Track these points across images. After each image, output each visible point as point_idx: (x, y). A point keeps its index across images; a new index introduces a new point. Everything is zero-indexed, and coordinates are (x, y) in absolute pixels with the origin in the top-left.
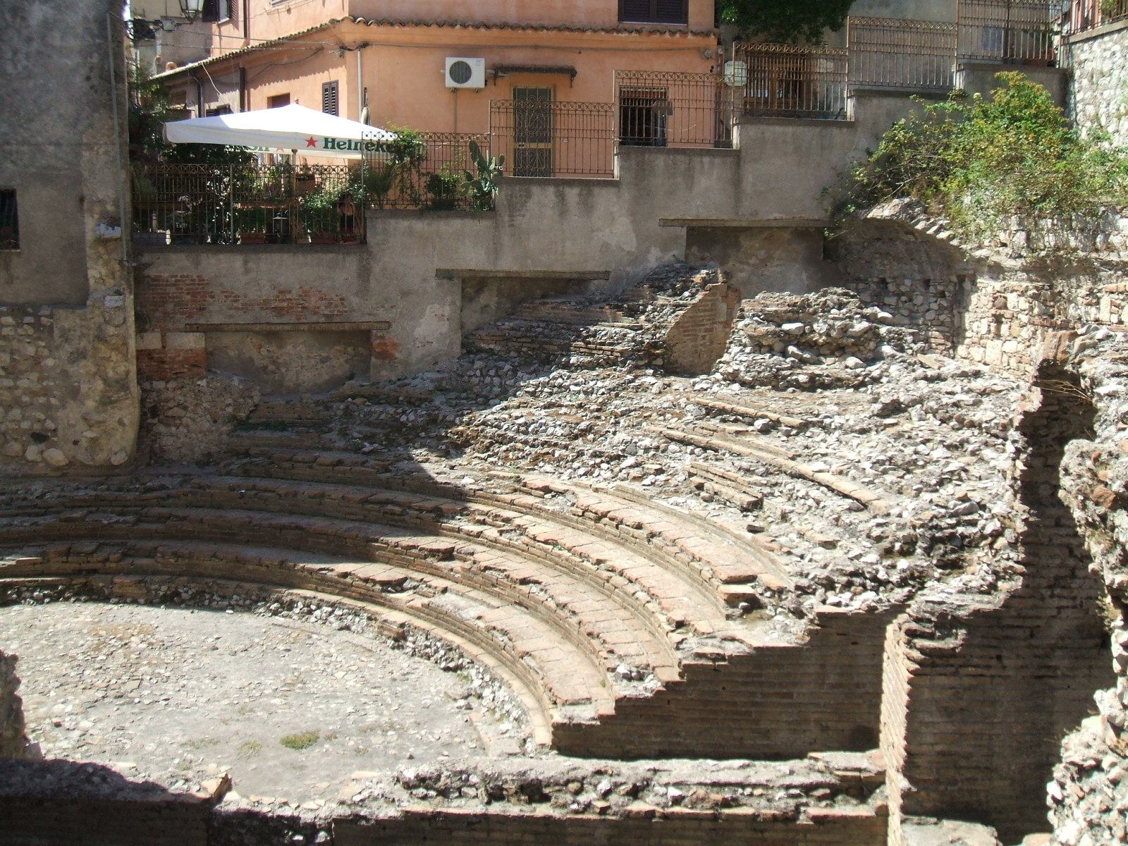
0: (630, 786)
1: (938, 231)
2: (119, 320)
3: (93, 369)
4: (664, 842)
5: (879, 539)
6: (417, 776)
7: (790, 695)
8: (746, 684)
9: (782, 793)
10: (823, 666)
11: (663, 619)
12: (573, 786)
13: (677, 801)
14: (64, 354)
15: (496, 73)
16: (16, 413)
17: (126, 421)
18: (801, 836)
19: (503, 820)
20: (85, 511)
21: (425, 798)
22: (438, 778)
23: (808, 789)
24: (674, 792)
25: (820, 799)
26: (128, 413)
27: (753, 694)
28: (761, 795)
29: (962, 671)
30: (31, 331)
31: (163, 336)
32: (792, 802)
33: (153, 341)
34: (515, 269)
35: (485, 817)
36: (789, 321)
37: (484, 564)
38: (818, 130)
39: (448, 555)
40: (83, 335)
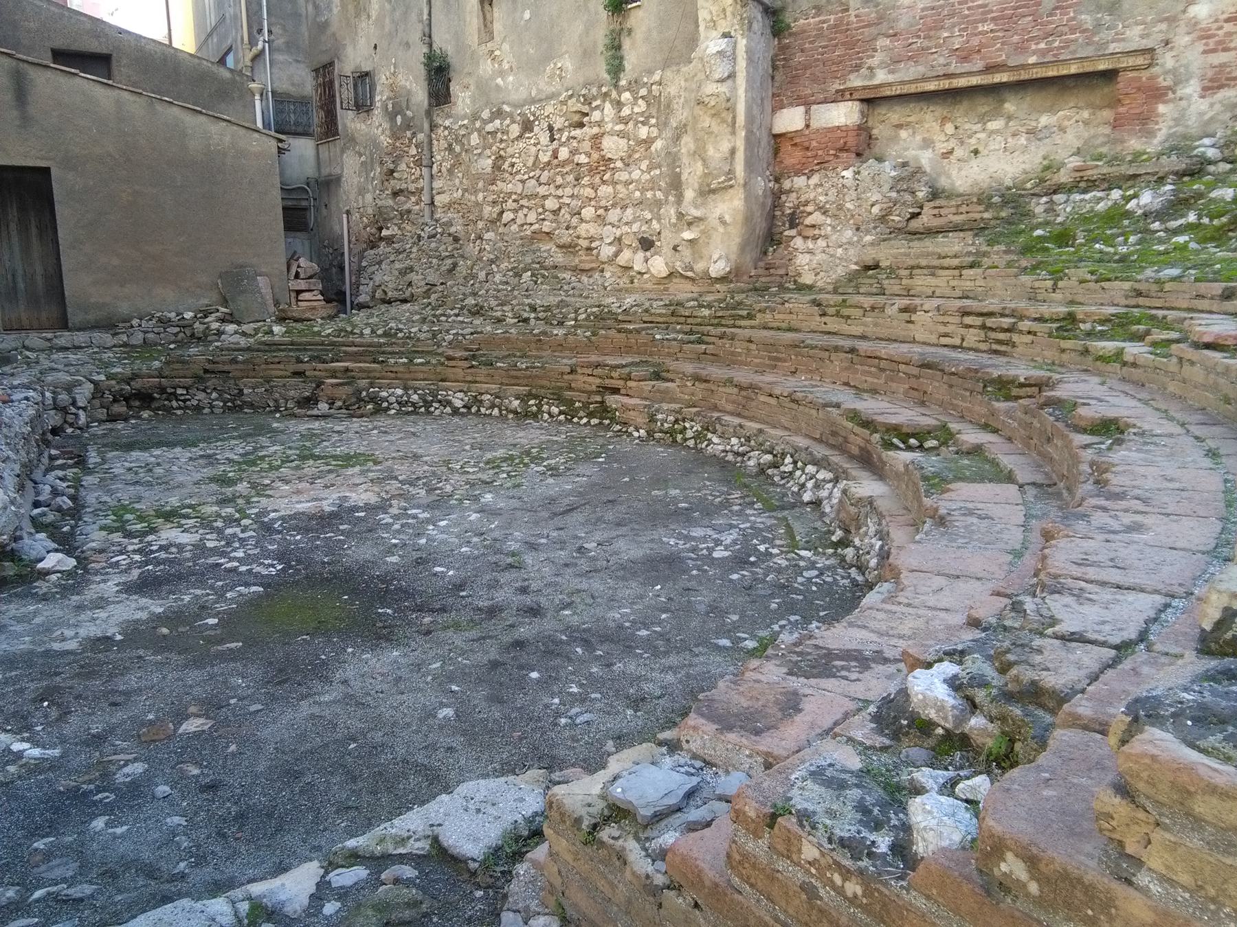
2: (721, 70)
14: (668, 133)
17: (727, 218)
31: (807, 112)
33: (790, 120)
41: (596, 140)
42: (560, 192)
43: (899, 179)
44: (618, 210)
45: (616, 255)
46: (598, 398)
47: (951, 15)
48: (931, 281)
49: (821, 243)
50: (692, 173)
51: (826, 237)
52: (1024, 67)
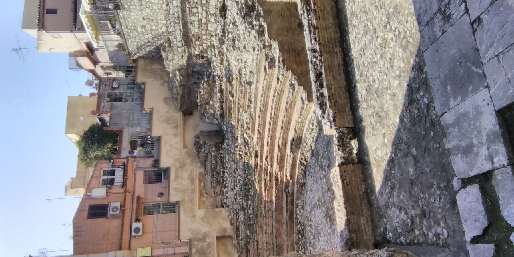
4: (326, 40)
5: (250, 32)
7: (291, 43)
9: (310, 16)
10: (282, 35)
11: (278, 85)
13: (315, 39)
15: (138, 220)
19: (327, 81)
22: (320, 103)
23: (308, 11)
24: (313, 42)
25: (310, 7)
35: (327, 85)
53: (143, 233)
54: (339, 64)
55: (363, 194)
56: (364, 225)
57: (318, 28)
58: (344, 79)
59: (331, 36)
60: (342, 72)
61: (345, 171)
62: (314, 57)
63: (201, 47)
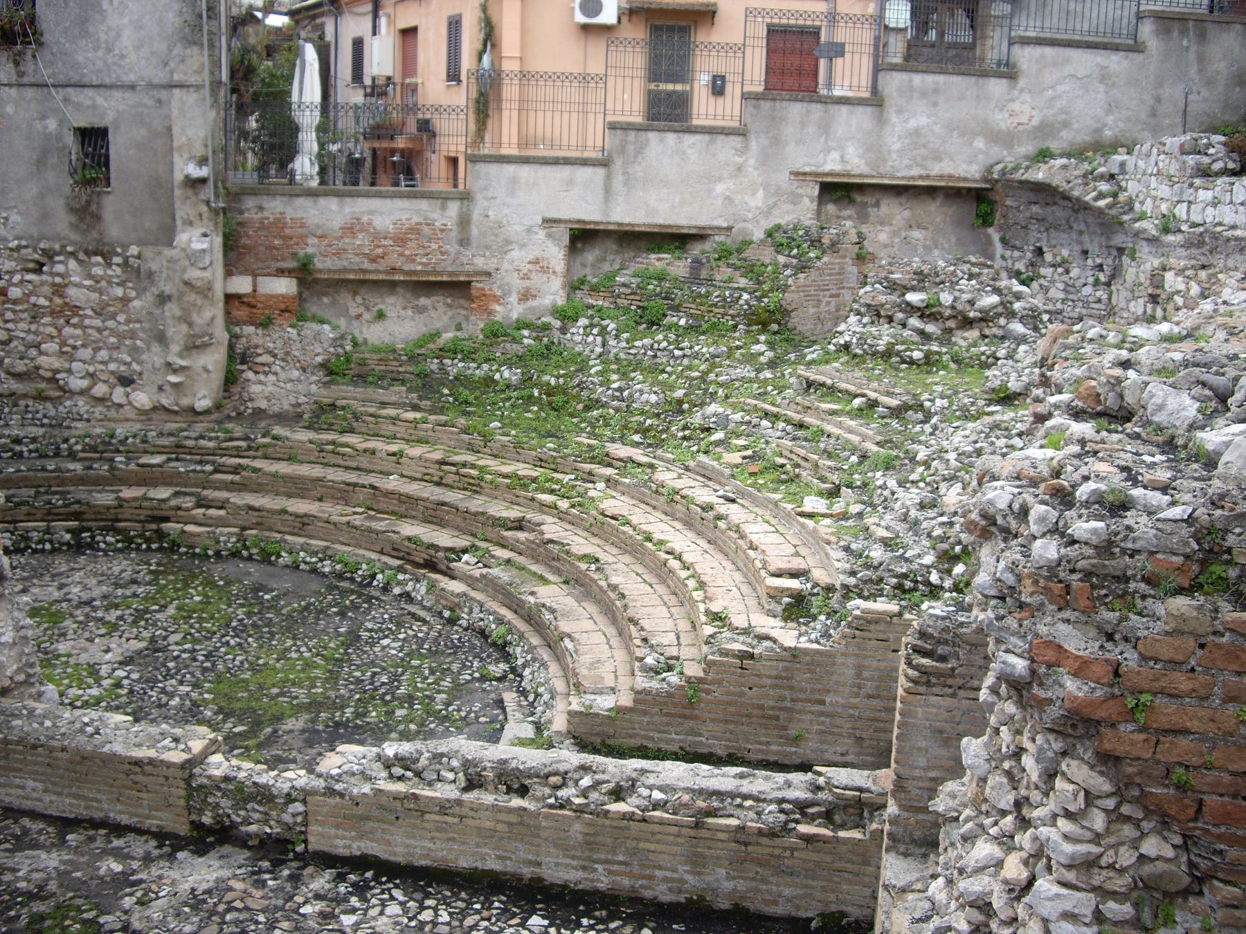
0: (612, 785)
1: (1096, 199)
3: (178, 313)
4: (642, 845)
6: (396, 755)
7: (822, 702)
8: (774, 687)
9: (773, 807)
10: (859, 675)
12: (553, 780)
13: (656, 806)
16: (103, 354)
17: (210, 367)
18: (788, 853)
19: (476, 808)
20: (164, 457)
21: (401, 778)
23: (802, 806)
24: (657, 795)
25: (811, 819)
26: (213, 360)
27: (783, 699)
28: (750, 808)
29: (962, 693)
30: (118, 270)
32: (782, 817)
33: (242, 284)
34: (627, 220)
36: (913, 289)
37: (547, 536)
38: (973, 79)
39: (519, 525)
40: (168, 278)
41: (59, 290)
42: (10, 326)
43: (335, 340)
44: (90, 350)
45: (91, 388)
46: (154, 526)
47: (361, 231)
48: (391, 427)
49: (272, 378)
50: (177, 333)
51: (276, 374)
52: (415, 273)
53: (586, 28)
54: (539, 864)
55: (102, 810)
56: (23, 787)
57: (698, 825)
58: (480, 865)
59: (660, 868)
60: (510, 867)
61: (167, 778)
62: (596, 785)
63: (1179, 300)
